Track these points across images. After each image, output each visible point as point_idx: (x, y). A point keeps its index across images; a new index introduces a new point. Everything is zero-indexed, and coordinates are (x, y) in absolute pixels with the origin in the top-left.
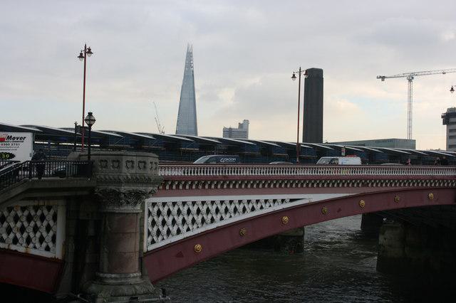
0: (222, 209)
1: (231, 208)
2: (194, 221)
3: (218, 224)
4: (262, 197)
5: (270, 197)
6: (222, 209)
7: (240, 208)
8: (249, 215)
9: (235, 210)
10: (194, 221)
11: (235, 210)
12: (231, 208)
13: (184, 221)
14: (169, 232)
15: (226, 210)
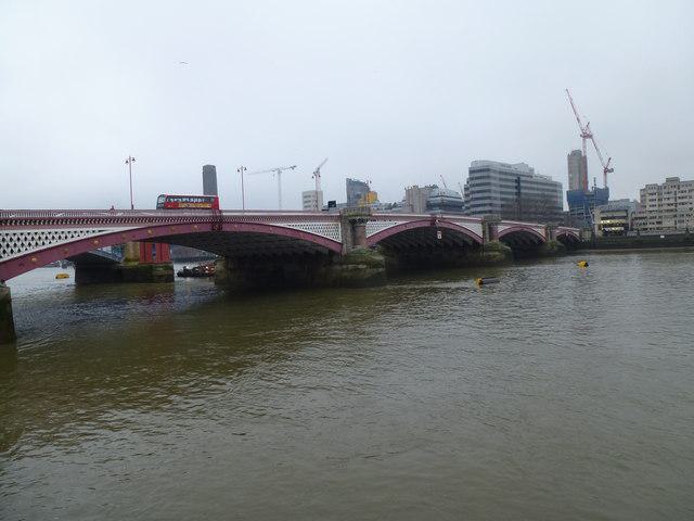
0: (50, 237)
1: (56, 236)
2: (30, 244)
3: (47, 246)
4: (78, 230)
5: (85, 229)
6: (50, 237)
7: (63, 236)
8: (70, 240)
9: (60, 238)
10: (30, 244)
11: (60, 238)
12: (56, 236)
13: (22, 245)
14: (12, 251)
15: (53, 238)
